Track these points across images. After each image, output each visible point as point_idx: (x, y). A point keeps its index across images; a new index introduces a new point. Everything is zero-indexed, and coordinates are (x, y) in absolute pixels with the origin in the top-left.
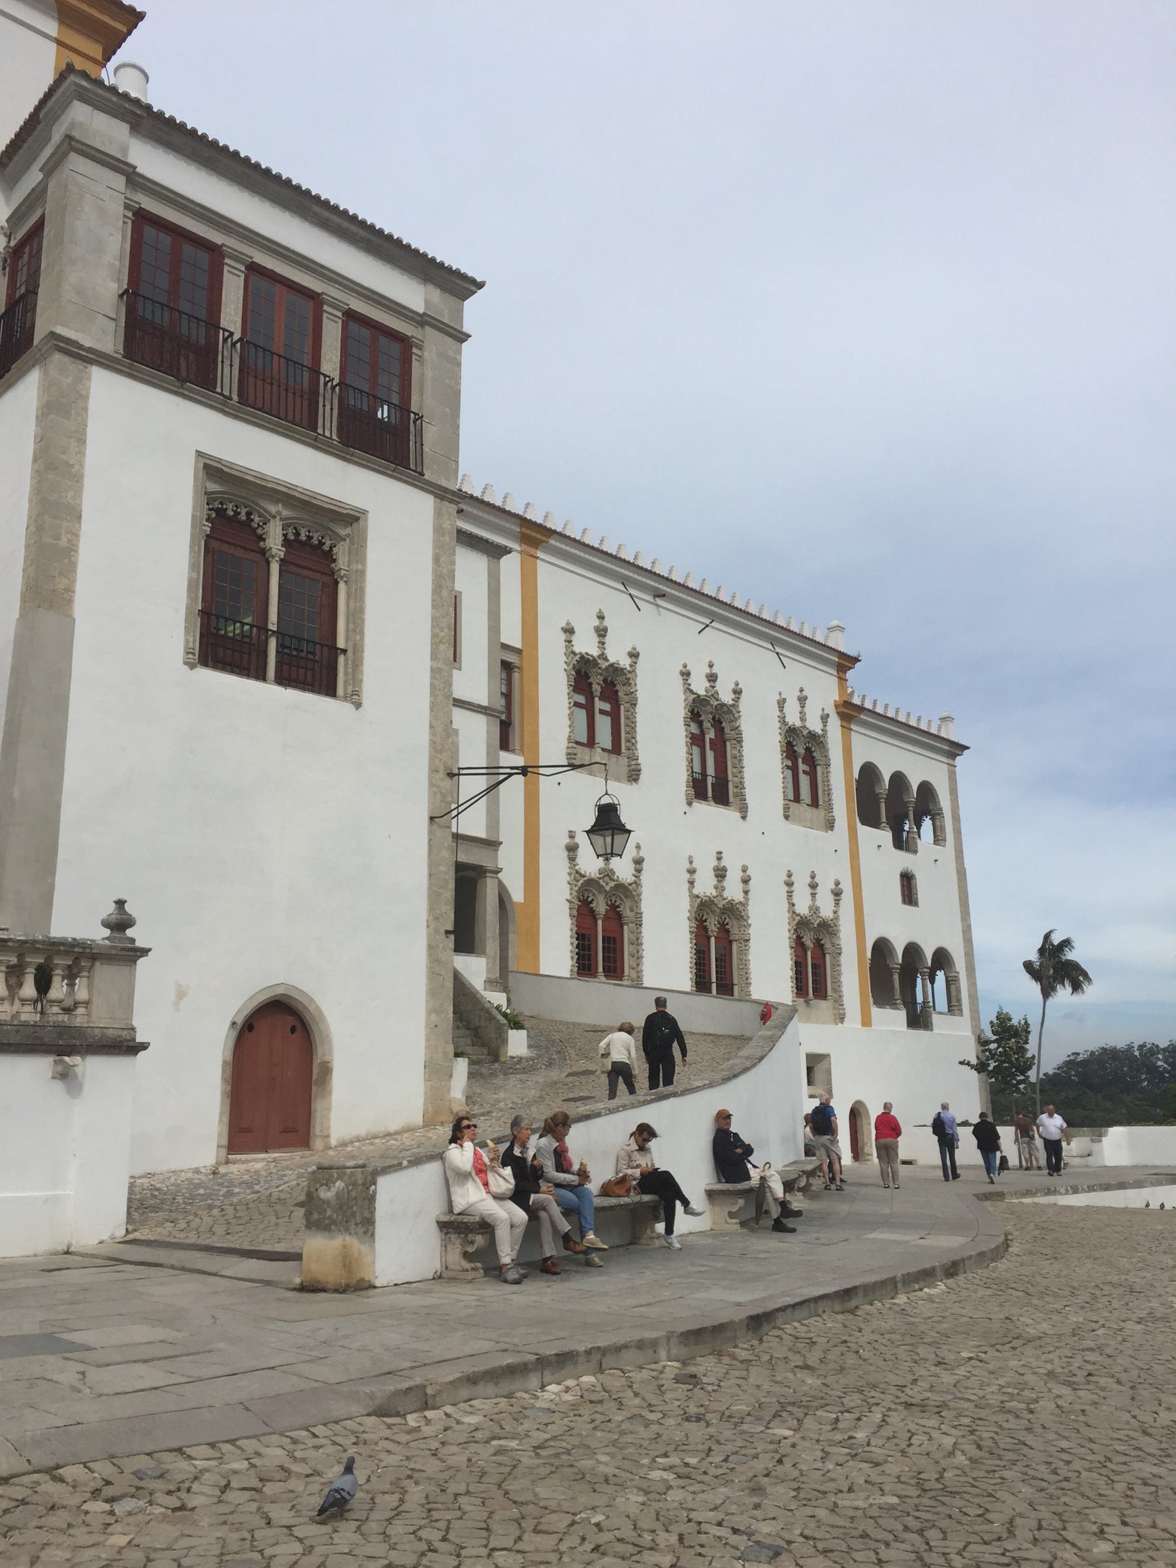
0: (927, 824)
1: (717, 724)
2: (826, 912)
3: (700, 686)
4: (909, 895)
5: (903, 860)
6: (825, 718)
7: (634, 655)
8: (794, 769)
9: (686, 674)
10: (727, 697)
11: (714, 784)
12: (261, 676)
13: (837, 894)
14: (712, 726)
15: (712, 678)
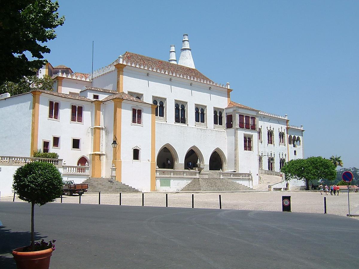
0: (298, 141)
1: (271, 133)
2: (284, 158)
3: (269, 129)
4: (295, 154)
5: (294, 149)
6: (284, 130)
7: (261, 126)
8: (280, 137)
9: (267, 127)
10: (272, 130)
11: (270, 141)
12: (247, 150)
13: (285, 155)
14: (270, 134)
15: (270, 127)
